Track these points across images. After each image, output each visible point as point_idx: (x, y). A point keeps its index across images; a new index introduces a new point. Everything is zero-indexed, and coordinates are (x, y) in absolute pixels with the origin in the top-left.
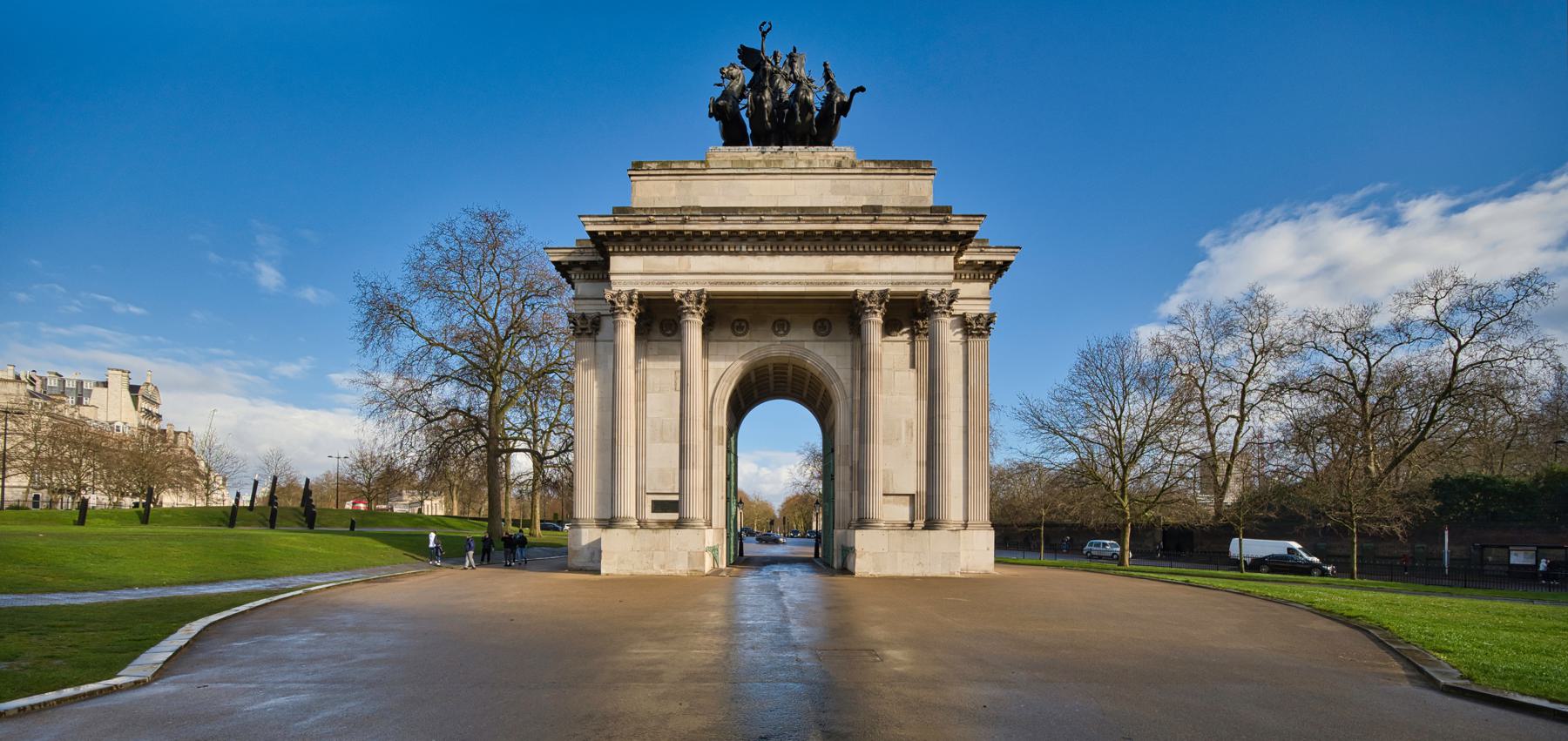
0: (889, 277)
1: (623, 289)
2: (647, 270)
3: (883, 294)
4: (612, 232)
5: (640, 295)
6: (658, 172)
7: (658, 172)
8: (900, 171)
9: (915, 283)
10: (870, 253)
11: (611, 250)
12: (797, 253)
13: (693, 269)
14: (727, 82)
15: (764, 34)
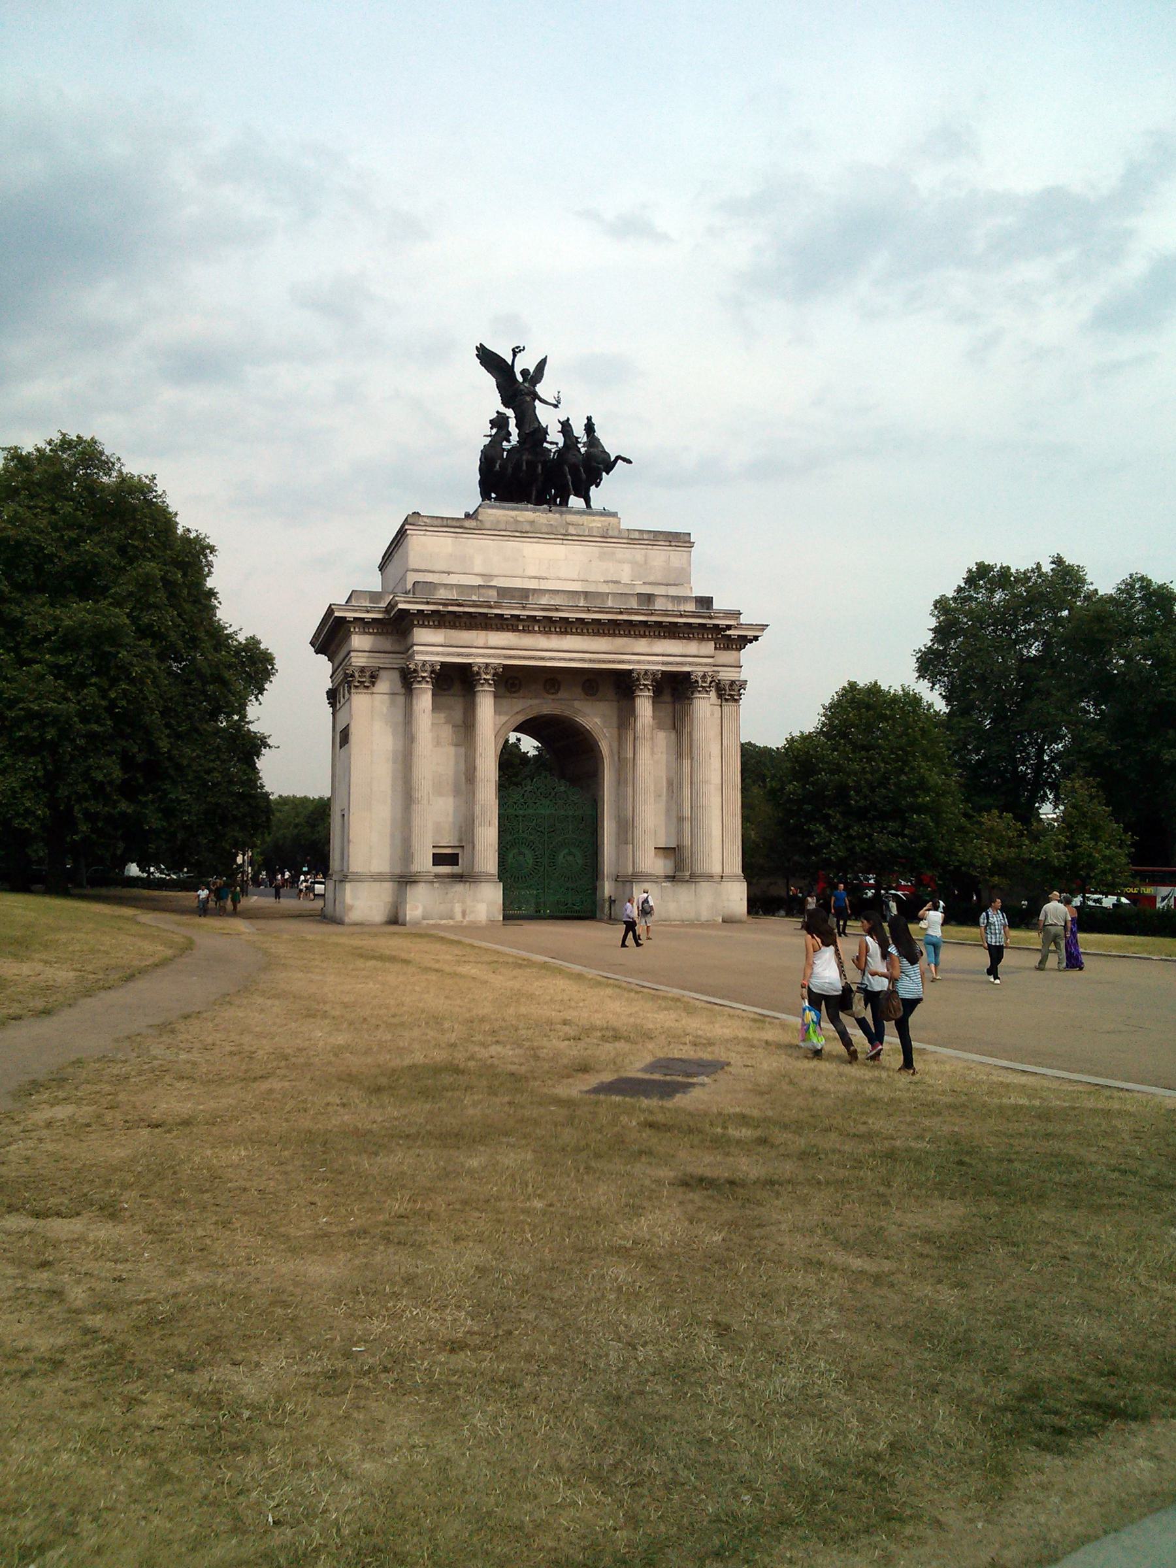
0: (660, 658)
1: (427, 658)
2: (449, 642)
3: (654, 673)
4: (423, 611)
5: (443, 664)
6: (436, 529)
7: (436, 529)
8: (663, 543)
9: (681, 664)
10: (644, 636)
11: (416, 623)
12: (582, 634)
13: (491, 643)
14: (494, 431)
15: (515, 355)
